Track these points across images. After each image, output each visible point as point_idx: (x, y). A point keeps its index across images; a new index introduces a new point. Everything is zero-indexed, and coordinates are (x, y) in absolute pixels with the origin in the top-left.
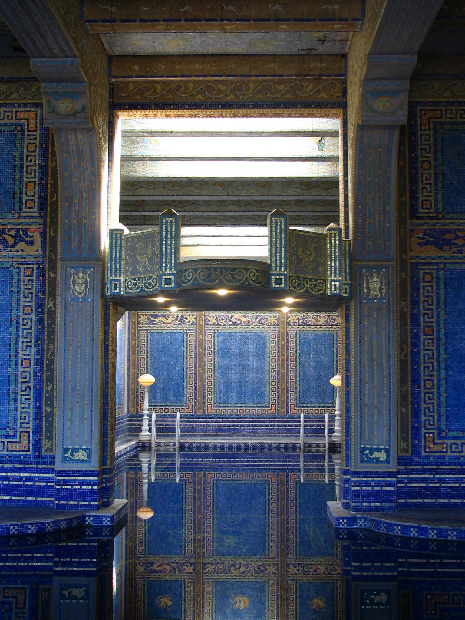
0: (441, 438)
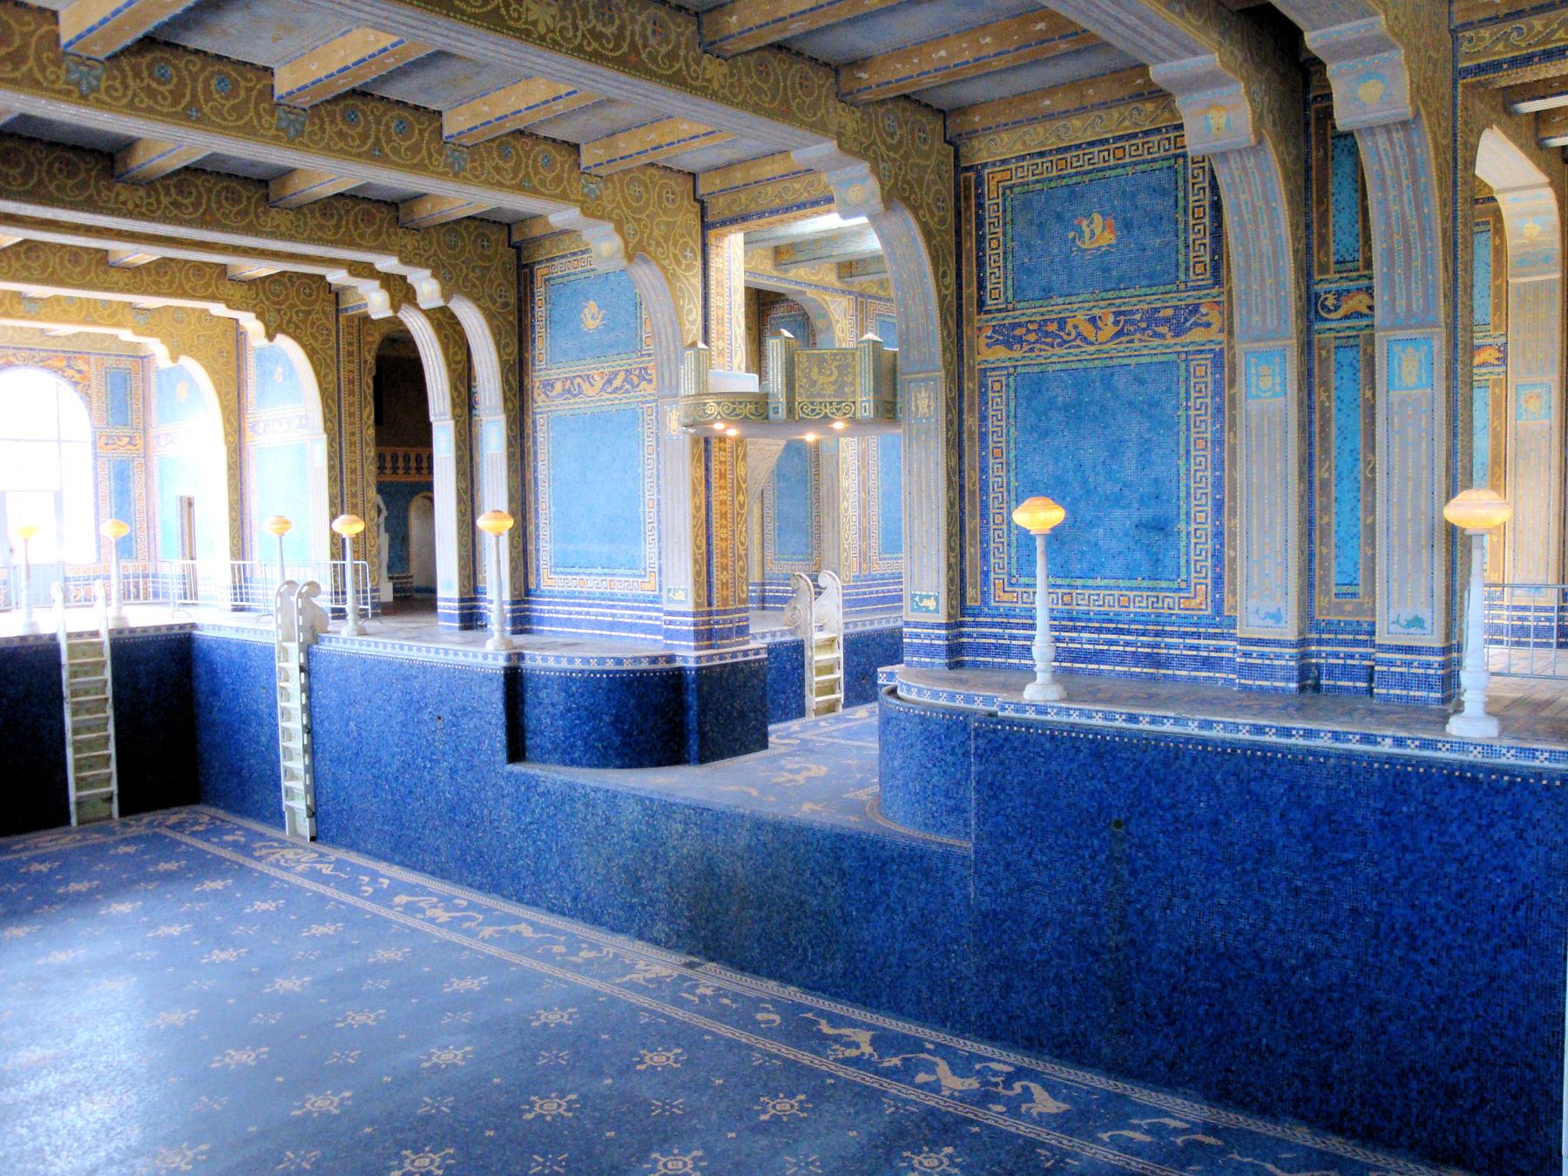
0: (1011, 585)
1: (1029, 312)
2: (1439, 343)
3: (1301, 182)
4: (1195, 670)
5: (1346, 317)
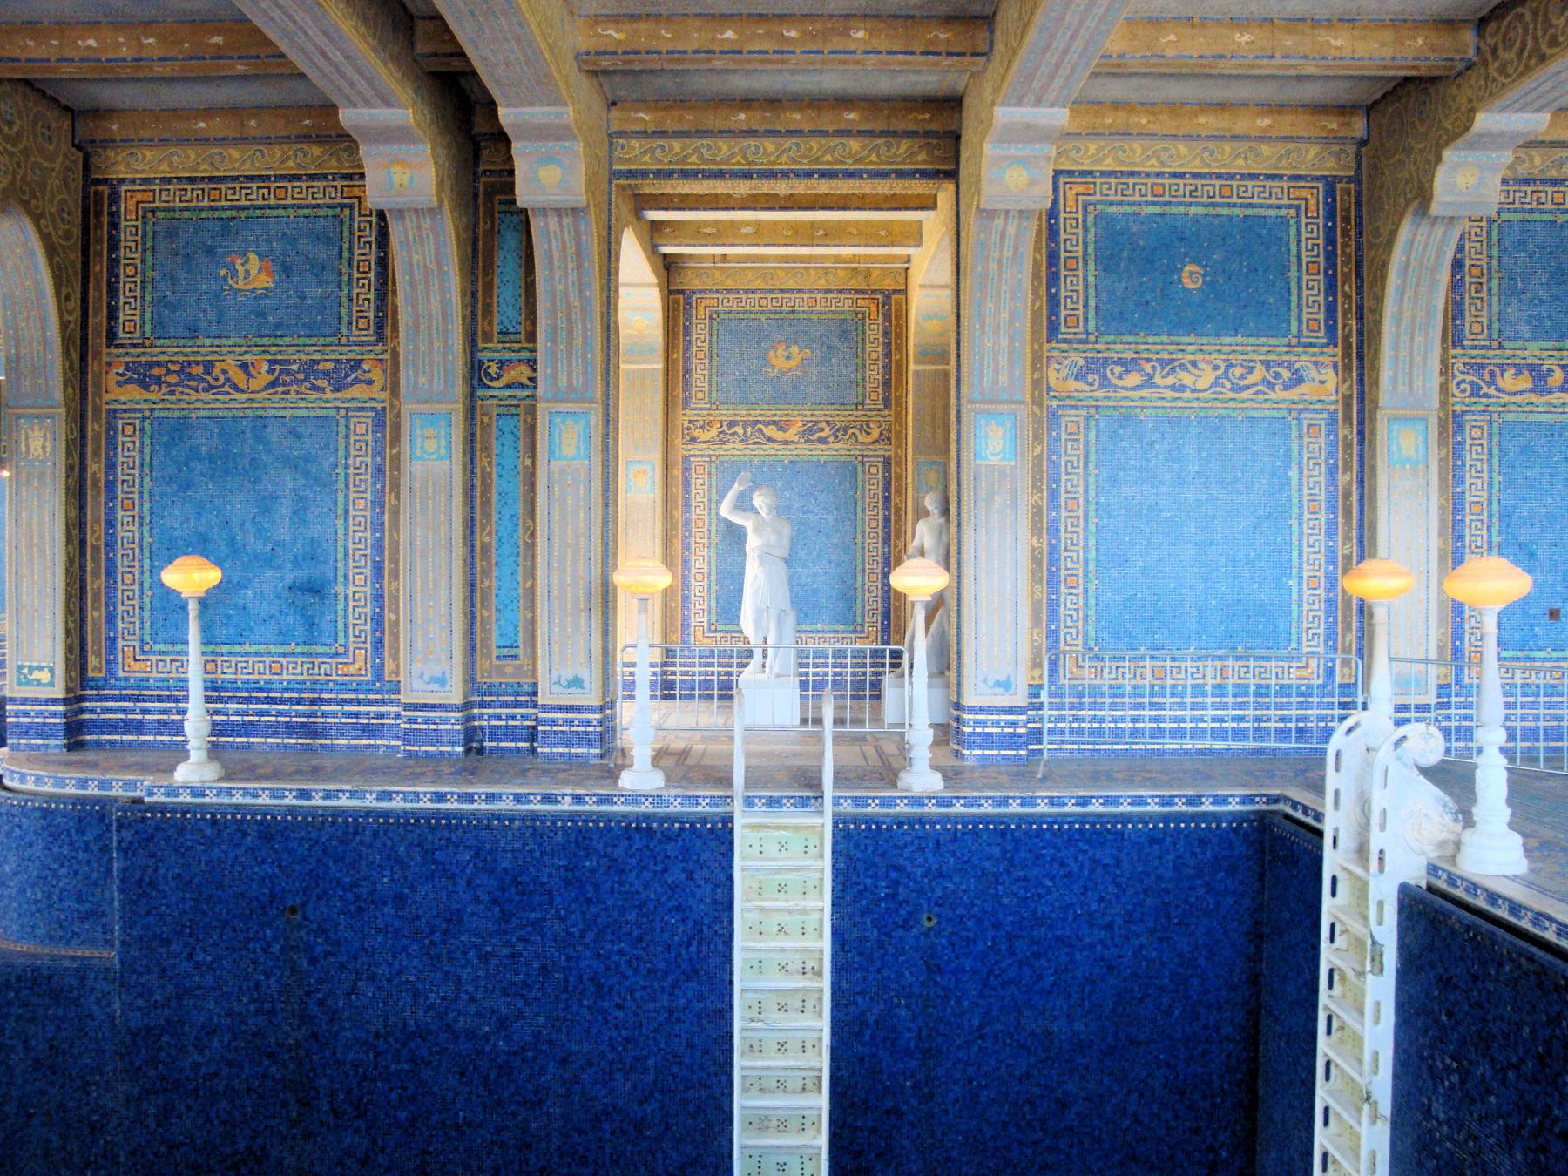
0: (144, 652)
1: (169, 351)
2: (596, 419)
3: (469, 250)
4: (355, 738)
5: (508, 386)
